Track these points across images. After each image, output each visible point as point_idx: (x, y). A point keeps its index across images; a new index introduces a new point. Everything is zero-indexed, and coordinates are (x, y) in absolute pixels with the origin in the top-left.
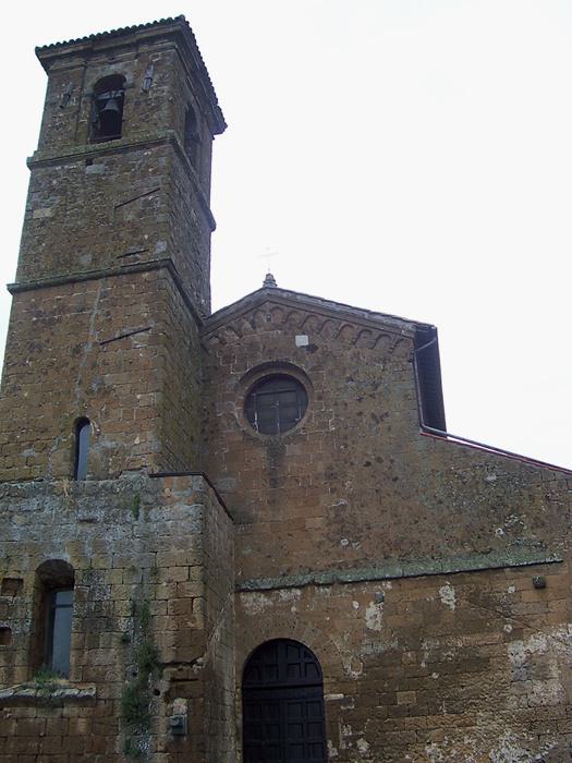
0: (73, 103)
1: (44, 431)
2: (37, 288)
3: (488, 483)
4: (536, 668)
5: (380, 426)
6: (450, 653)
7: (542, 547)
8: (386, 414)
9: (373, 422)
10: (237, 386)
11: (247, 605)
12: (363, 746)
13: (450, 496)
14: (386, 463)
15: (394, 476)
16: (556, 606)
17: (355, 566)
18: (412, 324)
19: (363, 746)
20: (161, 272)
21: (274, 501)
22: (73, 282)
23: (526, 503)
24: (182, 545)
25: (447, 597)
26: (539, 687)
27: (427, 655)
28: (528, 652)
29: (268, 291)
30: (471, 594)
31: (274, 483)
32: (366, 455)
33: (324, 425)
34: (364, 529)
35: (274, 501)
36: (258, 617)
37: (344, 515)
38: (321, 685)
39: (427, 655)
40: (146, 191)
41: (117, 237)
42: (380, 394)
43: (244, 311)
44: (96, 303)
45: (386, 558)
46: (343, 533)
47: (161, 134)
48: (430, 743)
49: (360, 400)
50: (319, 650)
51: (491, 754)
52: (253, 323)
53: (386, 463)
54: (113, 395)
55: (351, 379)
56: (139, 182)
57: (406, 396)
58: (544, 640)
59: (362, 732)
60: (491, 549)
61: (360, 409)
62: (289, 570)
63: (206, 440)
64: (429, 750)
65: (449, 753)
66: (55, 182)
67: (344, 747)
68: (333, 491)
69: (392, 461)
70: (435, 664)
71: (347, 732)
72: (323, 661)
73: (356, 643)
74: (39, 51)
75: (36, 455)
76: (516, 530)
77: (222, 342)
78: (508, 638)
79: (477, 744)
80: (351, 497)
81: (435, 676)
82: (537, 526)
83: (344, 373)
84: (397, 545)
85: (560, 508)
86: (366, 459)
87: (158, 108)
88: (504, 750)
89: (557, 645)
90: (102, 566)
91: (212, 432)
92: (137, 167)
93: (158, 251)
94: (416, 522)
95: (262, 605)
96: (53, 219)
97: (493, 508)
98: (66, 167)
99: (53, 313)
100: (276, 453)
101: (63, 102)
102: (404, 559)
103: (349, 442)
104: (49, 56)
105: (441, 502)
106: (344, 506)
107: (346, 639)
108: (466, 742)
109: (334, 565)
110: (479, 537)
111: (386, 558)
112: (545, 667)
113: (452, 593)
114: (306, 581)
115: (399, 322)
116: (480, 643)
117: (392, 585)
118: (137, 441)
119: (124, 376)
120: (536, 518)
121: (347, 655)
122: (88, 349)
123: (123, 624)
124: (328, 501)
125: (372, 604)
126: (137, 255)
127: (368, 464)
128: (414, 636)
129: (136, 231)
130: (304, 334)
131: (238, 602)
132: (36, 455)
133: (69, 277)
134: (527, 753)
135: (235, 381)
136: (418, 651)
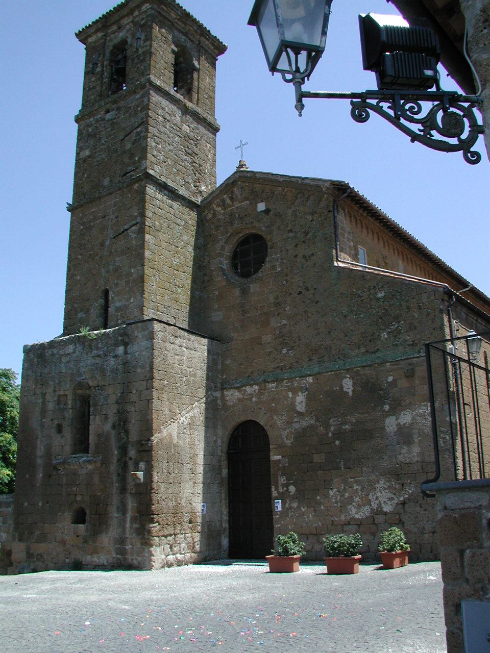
0: (99, 69)
1: (87, 300)
2: (82, 206)
3: (378, 299)
4: (405, 435)
5: (308, 263)
8: (313, 254)
9: (305, 262)
10: (222, 246)
11: (227, 398)
17: (290, 368)
18: (329, 183)
19: (292, 489)
27: (332, 428)
29: (238, 174)
31: (244, 312)
33: (274, 267)
36: (234, 406)
38: (269, 450)
39: (332, 428)
42: (309, 239)
45: (310, 360)
46: (284, 344)
49: (296, 246)
51: (370, 497)
52: (231, 199)
55: (291, 231)
56: (133, 119)
57: (326, 239)
58: (410, 416)
60: (378, 350)
64: (331, 493)
65: (343, 496)
66: (90, 130)
67: (281, 491)
68: (278, 314)
69: (315, 289)
70: (339, 434)
71: (283, 480)
72: (271, 434)
73: (289, 423)
74: (78, 35)
75: (84, 316)
77: (214, 215)
79: (362, 490)
81: (337, 443)
85: (428, 314)
88: (379, 494)
91: (209, 281)
92: (132, 108)
94: (329, 333)
96: (89, 156)
97: (381, 318)
98: (95, 117)
99: (90, 222)
100: (245, 292)
103: (288, 278)
104: (83, 36)
106: (285, 324)
108: (355, 488)
109: (278, 367)
111: (310, 360)
115: (320, 183)
117: (313, 379)
118: (132, 301)
122: (108, 243)
124: (274, 323)
125: (300, 393)
126: (132, 173)
127: (300, 293)
130: (262, 201)
131: (223, 396)
132: (84, 316)
134: (393, 496)
135: (221, 244)
136: (327, 426)
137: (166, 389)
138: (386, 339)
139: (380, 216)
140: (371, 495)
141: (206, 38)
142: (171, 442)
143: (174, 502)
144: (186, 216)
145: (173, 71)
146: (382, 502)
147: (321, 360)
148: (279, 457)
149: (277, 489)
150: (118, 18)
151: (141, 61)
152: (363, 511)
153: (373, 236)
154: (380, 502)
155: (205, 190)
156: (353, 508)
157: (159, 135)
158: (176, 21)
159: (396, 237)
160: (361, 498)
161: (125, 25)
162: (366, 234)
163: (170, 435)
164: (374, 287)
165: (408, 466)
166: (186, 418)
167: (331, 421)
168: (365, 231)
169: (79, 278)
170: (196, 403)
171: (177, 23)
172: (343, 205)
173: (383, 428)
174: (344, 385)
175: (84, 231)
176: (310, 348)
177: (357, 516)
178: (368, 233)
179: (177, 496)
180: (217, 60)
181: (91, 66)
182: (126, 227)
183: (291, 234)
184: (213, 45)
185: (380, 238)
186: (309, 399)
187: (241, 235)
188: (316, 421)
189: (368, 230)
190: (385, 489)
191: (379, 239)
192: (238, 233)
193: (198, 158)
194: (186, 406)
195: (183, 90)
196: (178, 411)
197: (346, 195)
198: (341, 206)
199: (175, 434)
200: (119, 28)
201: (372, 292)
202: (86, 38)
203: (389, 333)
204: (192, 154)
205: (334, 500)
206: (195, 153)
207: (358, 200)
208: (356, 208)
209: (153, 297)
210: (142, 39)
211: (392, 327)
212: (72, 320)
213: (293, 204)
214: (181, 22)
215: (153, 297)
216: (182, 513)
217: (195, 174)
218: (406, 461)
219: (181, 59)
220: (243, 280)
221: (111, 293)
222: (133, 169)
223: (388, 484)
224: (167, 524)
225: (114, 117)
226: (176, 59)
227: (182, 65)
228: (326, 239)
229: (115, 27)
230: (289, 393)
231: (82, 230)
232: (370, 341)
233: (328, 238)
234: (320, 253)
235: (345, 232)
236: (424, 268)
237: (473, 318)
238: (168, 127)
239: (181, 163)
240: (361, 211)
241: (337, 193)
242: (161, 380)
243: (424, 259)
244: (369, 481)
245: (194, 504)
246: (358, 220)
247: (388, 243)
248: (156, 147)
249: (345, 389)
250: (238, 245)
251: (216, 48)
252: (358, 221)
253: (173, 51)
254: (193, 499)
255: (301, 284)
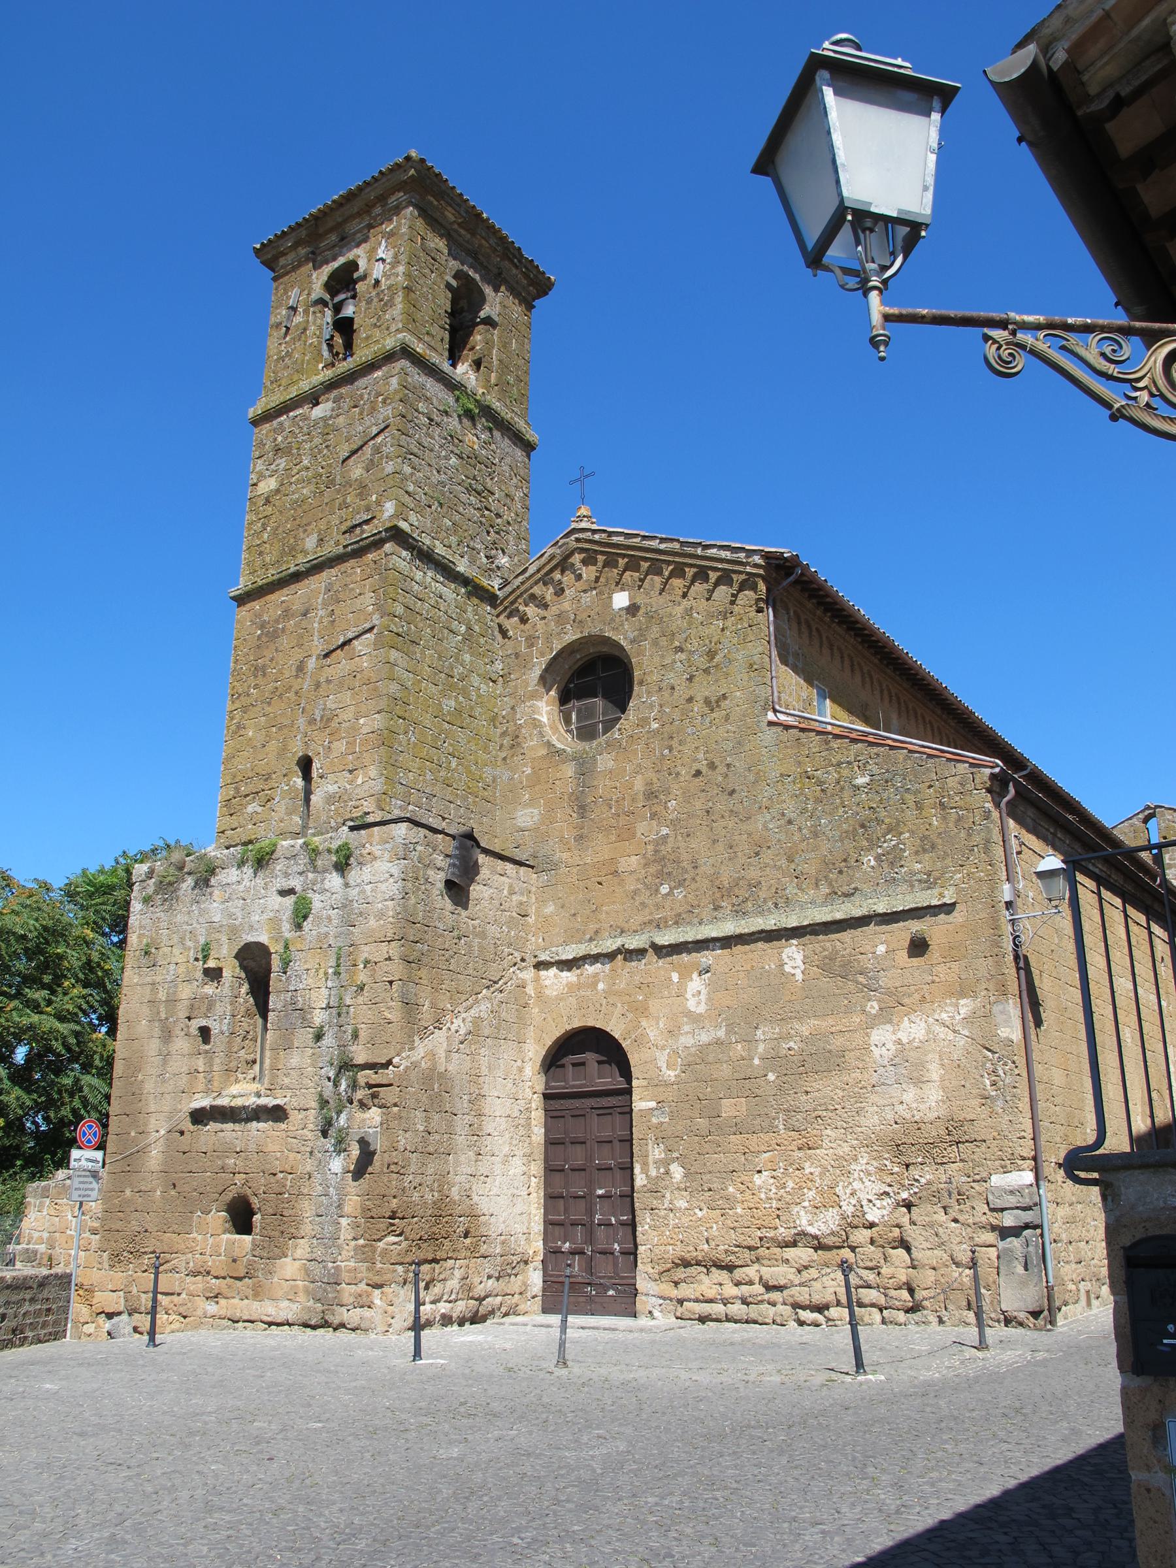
5: (714, 715)
6: (792, 1044)
7: (929, 883)
8: (724, 697)
9: (706, 710)
11: (547, 982)
12: (677, 1172)
13: (804, 811)
14: (722, 769)
15: (730, 787)
16: (946, 972)
17: (676, 923)
19: (677, 1172)
20: (388, 547)
21: (581, 837)
22: (297, 577)
23: (910, 814)
24: (381, 915)
25: (791, 963)
26: (910, 1095)
27: (761, 1048)
28: (899, 1042)
30: (826, 957)
31: (582, 810)
32: (695, 760)
33: (644, 722)
34: (689, 867)
35: (581, 837)
37: (665, 849)
39: (761, 1048)
40: (375, 430)
41: (344, 505)
43: (548, 568)
44: (320, 601)
46: (662, 876)
47: (390, 343)
48: (759, 1172)
49: (690, 679)
50: (629, 1042)
53: (722, 769)
54: (334, 724)
55: (680, 649)
56: (368, 420)
57: (751, 665)
58: (923, 1025)
59: (675, 1155)
60: (856, 889)
61: (691, 693)
62: (597, 932)
63: (504, 759)
64: (758, 1180)
65: (784, 1186)
66: (280, 439)
68: (654, 816)
69: (728, 766)
70: (773, 1060)
71: (656, 1153)
76: (893, 858)
78: (873, 1022)
79: (821, 1175)
80: (674, 824)
81: (771, 1077)
82: (925, 851)
83: (672, 641)
84: (725, 892)
85: (960, 819)
86: (696, 766)
87: (390, 304)
89: (942, 1032)
90: (299, 946)
92: (366, 396)
93: (387, 515)
94: (757, 854)
95: (564, 982)
96: (278, 491)
97: (863, 826)
98: (291, 414)
100: (585, 768)
101: (288, 319)
102: (739, 912)
103: (675, 743)
105: (790, 822)
107: (661, 1025)
108: (807, 1171)
109: (650, 922)
110: (841, 872)
111: (715, 909)
112: (921, 1065)
113: (799, 957)
114: (614, 947)
116: (833, 1029)
119: (347, 697)
120: (924, 838)
121: (663, 1048)
122: (312, 663)
123: (319, 1017)
124: (645, 829)
127: (698, 773)
128: (751, 1017)
129: (363, 489)
131: (537, 980)
132: (259, 809)
133: (290, 571)
134: (888, 1189)
136: (750, 1041)
137: (425, 960)
138: (873, 867)
139: (857, 622)
140: (840, 1187)
141: (512, 262)
142: (433, 1069)
143: (436, 1194)
144: (470, 615)
145: (447, 327)
146: (864, 1203)
147: (739, 908)
148: (653, 1104)
149: (645, 1171)
150: (340, 220)
151: (386, 304)
152: (824, 1220)
153: (842, 662)
154: (859, 1201)
155: (507, 565)
156: (802, 1213)
157: (420, 453)
158: (456, 226)
159: (887, 665)
160: (821, 1193)
161: (355, 234)
162: (829, 659)
163: (432, 1055)
164: (849, 763)
165: (919, 1129)
166: (464, 1020)
167: (759, 1032)
168: (826, 651)
169: (250, 734)
170: (484, 991)
171: (456, 231)
172: (785, 599)
173: (867, 1049)
174: (786, 960)
175: (264, 639)
176: (717, 883)
177: (812, 1230)
178: (832, 655)
179: (442, 1179)
180: (534, 307)
181: (284, 312)
182: (350, 635)
183: (683, 656)
184: (526, 276)
185: (856, 667)
186: (714, 988)
187: (578, 657)
188: (728, 1033)
189: (831, 649)
190: (870, 1174)
191: (852, 671)
192: (573, 652)
193: (493, 501)
194: (464, 997)
195: (466, 364)
196: (449, 1006)
197: (792, 578)
198: (781, 600)
199: (441, 1053)
200: (343, 239)
201: (845, 772)
202: (276, 258)
203: (878, 858)
204: (483, 493)
205: (763, 1196)
206: (489, 491)
207: (815, 589)
208: (809, 605)
209: (401, 775)
210: (388, 261)
211: (885, 845)
212: (234, 817)
213: (685, 595)
214: (466, 230)
215: (401, 775)
216: (451, 1215)
217: (488, 533)
218: (913, 1116)
219: (463, 303)
220: (581, 746)
221: (316, 765)
222: (366, 518)
223: (875, 1163)
224: (420, 1239)
225: (328, 413)
226: (454, 302)
227: (464, 314)
228: (751, 665)
229: (333, 238)
230: (672, 974)
231: (259, 637)
232: (841, 872)
233: (755, 663)
234: (738, 693)
235: (788, 653)
236: (939, 728)
237: (1048, 830)
238: (437, 438)
239: (461, 510)
240: (819, 612)
241: (774, 575)
242: (417, 942)
243: (939, 712)
244: (838, 1158)
245: (475, 1198)
246: (814, 629)
247: (871, 678)
248: (412, 474)
249: (787, 969)
250: (573, 675)
251: (532, 283)
252: (814, 633)
253: (448, 286)
254: (474, 1188)
255: (701, 756)
